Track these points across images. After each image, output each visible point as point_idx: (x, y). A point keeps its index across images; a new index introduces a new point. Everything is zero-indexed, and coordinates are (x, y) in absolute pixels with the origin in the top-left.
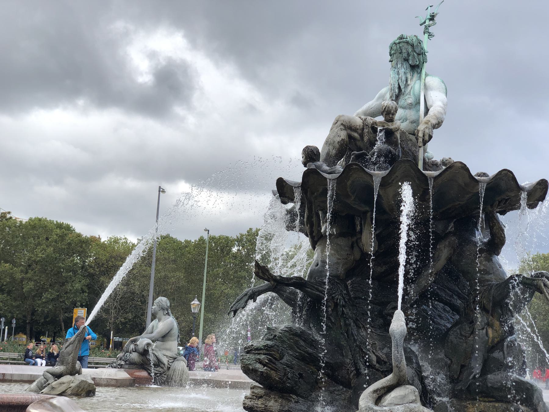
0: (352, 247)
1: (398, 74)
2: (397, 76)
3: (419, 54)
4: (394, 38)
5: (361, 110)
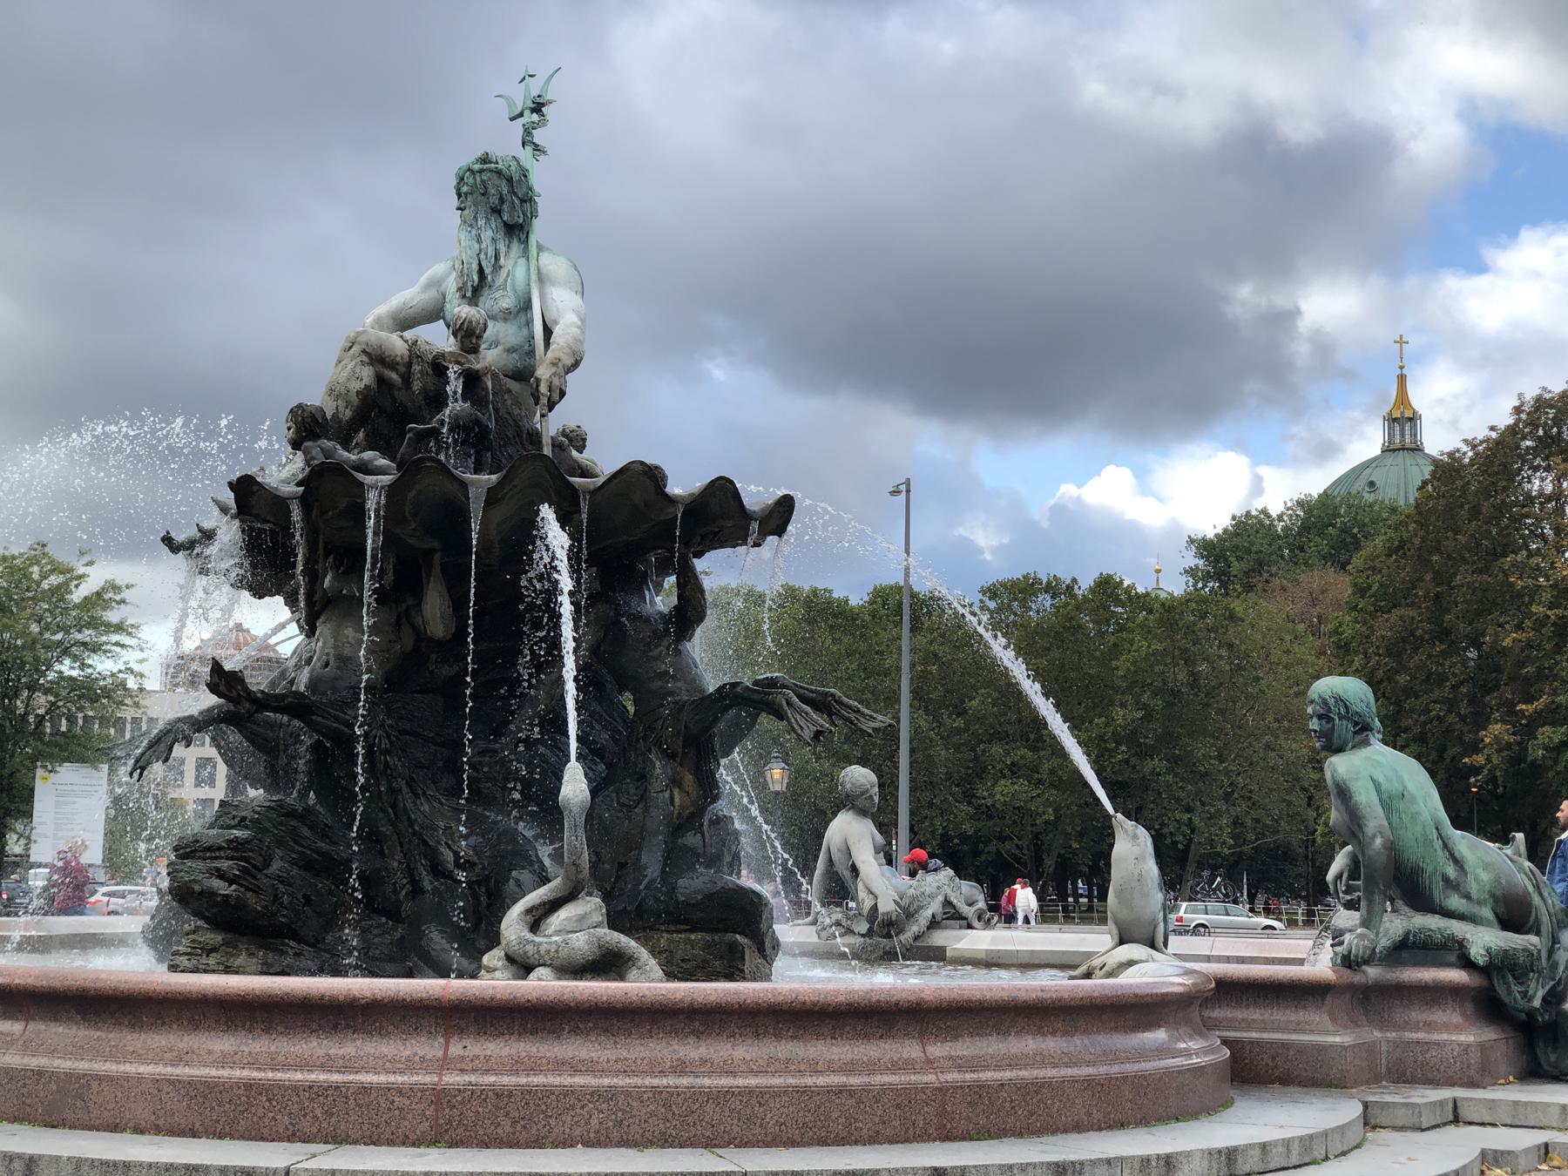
0: (398, 624)
1: (479, 240)
3: (523, 201)
4: (469, 158)
5: (382, 310)
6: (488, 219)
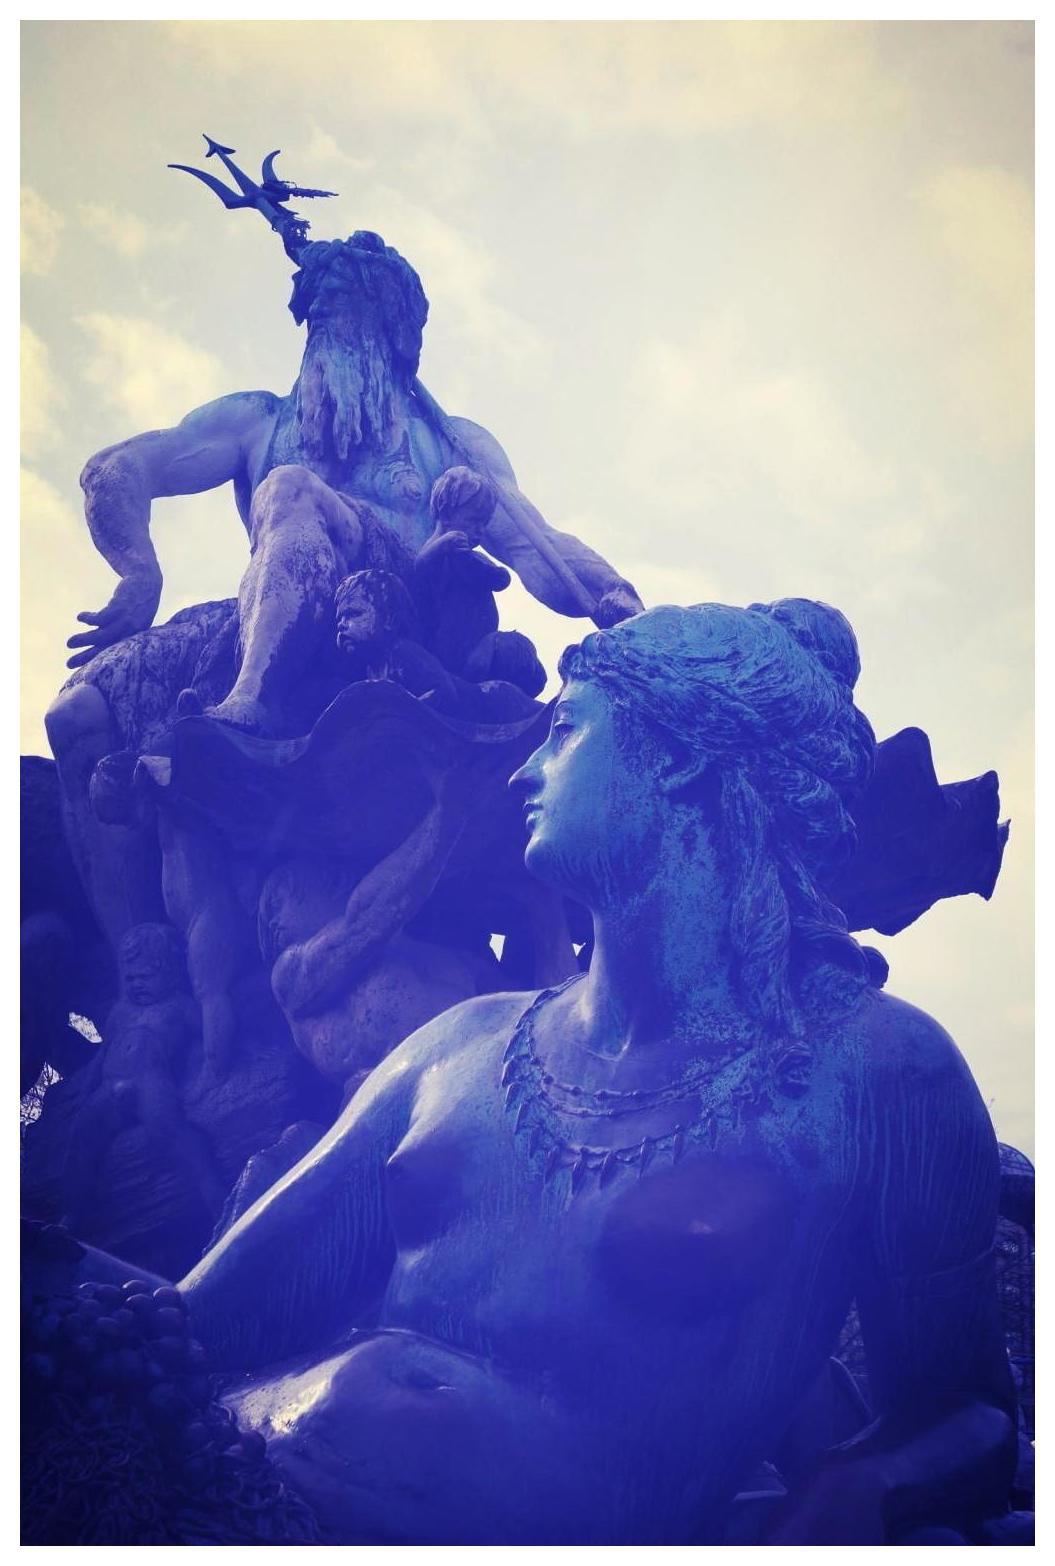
1: (365, 373)
2: (361, 381)
6: (378, 344)
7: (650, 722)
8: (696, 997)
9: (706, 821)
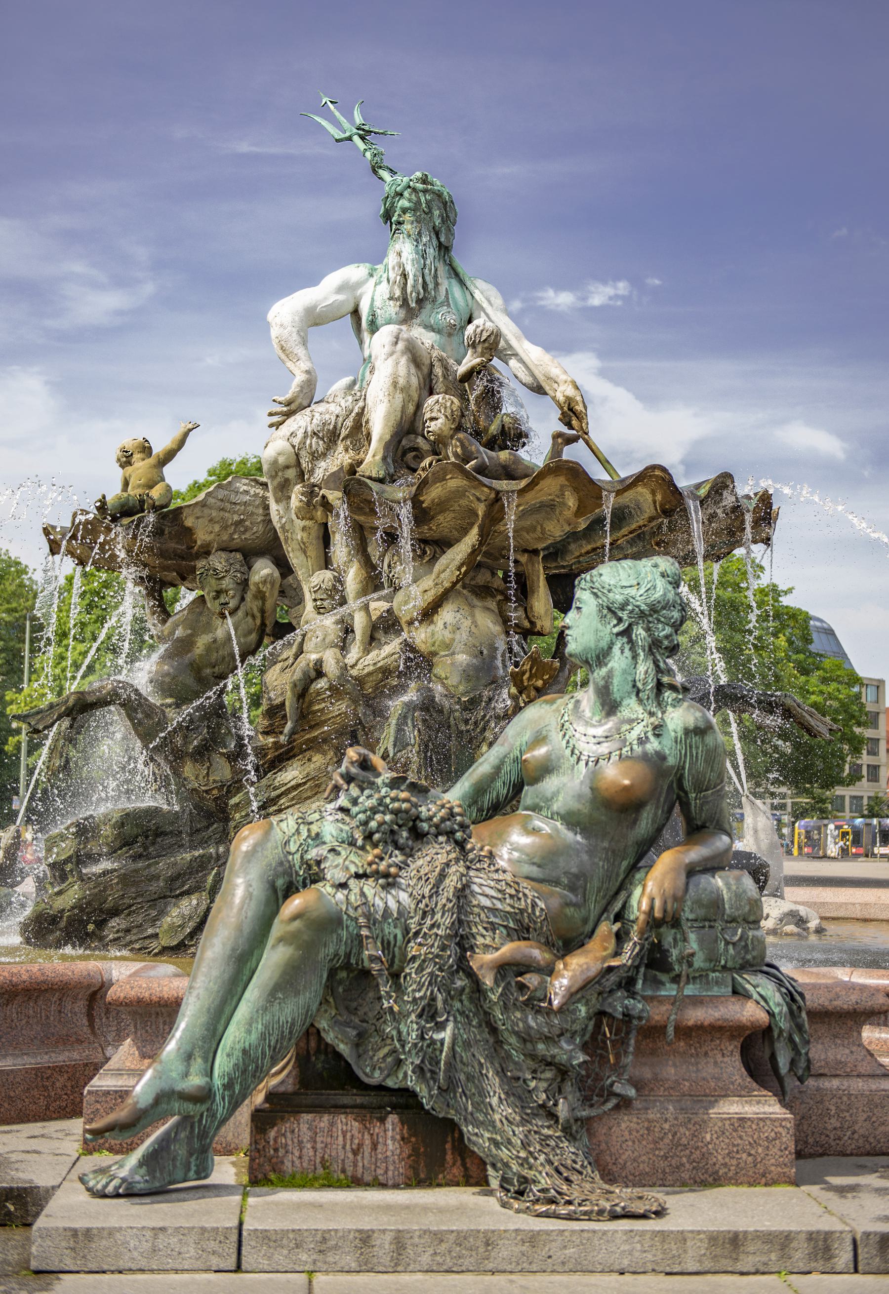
7: (609, 609)
8: (625, 703)
9: (628, 643)
